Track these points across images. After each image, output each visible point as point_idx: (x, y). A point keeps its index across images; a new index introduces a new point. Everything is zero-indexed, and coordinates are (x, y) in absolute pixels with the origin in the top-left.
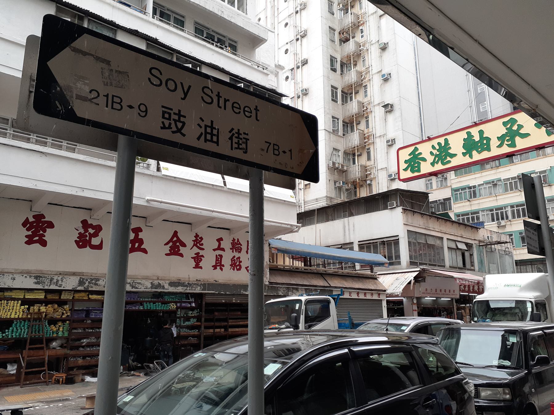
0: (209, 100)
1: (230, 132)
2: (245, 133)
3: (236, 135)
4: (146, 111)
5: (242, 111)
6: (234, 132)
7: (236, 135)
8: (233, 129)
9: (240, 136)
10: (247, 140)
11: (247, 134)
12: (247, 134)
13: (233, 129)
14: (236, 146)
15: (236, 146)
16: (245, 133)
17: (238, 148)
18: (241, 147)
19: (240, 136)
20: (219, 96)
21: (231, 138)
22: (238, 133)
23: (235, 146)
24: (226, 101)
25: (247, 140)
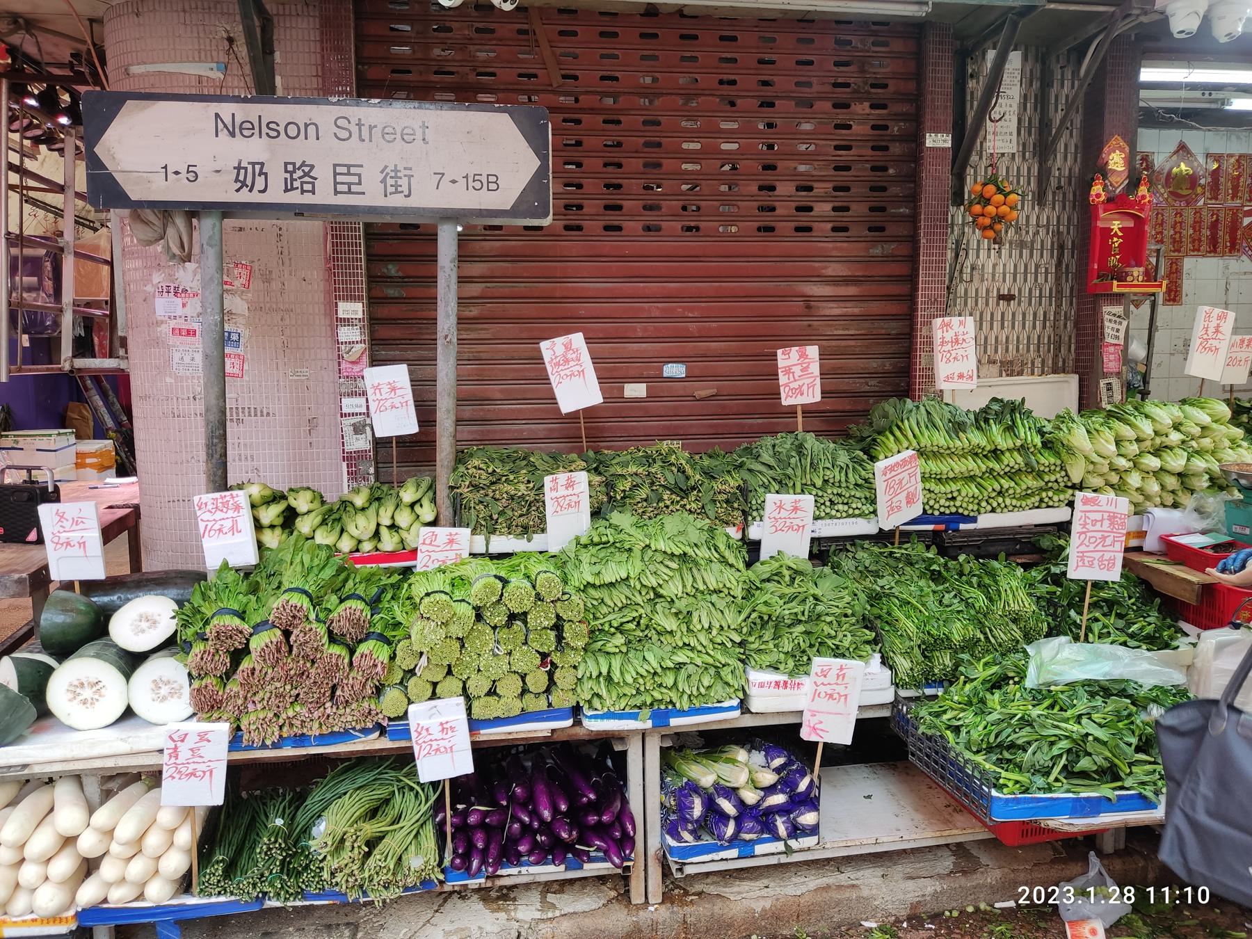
0: (344, 134)
1: (382, 172)
5: (398, 136)
6: (388, 170)
7: (393, 174)
8: (386, 167)
10: (410, 177)
13: (386, 167)
14: (393, 189)
15: (393, 189)
17: (397, 192)
20: (359, 125)
21: (384, 181)
22: (396, 171)
23: (390, 189)
24: (371, 128)
25: (410, 177)
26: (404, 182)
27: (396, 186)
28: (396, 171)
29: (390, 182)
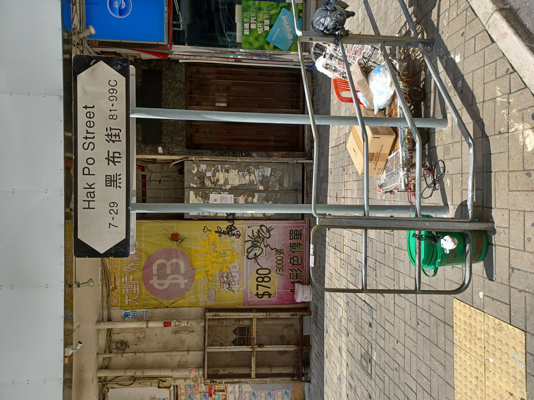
1: (109, 142)
2: (107, 131)
3: (110, 137)
4: (113, 203)
6: (108, 139)
7: (110, 137)
8: (106, 140)
9: (110, 134)
10: (111, 129)
11: (107, 128)
12: (107, 128)
13: (106, 140)
14: (117, 137)
15: (117, 137)
16: (107, 131)
18: (117, 134)
19: (110, 134)
21: (113, 141)
22: (108, 135)
23: (117, 139)
25: (111, 129)
26: (114, 132)
27: (115, 136)
28: (108, 135)
29: (114, 138)
